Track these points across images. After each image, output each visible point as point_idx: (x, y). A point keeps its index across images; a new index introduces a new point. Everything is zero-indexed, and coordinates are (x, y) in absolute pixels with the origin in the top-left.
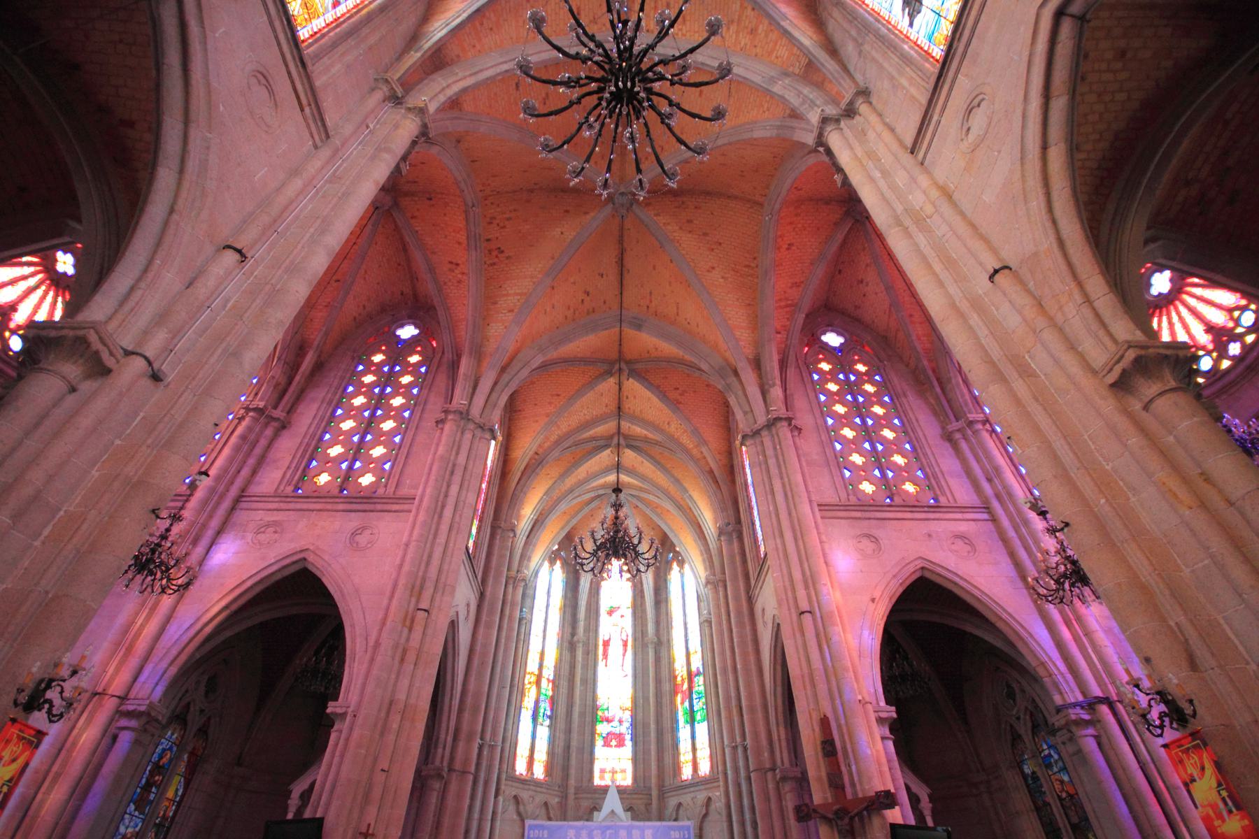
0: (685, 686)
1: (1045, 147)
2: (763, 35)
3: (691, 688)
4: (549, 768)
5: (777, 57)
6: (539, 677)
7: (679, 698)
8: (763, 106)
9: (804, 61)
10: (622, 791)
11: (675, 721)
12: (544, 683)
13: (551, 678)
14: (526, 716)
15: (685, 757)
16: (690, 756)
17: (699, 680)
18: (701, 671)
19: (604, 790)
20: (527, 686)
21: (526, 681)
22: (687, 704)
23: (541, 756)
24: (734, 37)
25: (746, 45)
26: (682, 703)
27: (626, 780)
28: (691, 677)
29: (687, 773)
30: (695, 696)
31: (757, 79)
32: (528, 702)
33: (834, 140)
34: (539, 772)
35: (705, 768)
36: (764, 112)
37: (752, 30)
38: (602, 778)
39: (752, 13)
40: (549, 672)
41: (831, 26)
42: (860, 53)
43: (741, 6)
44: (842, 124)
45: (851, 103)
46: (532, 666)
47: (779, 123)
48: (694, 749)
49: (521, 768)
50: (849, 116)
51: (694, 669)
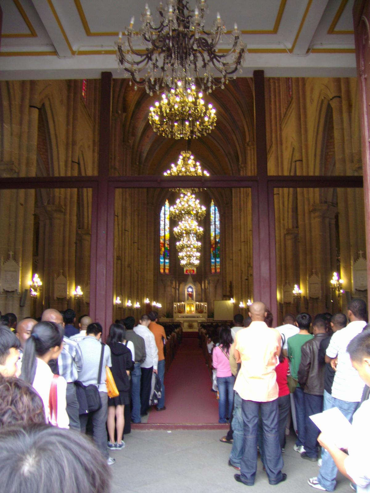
0: (214, 246)
3: (216, 246)
4: (170, 270)
6: (164, 244)
7: (212, 249)
10: (192, 275)
11: (210, 256)
12: (166, 245)
13: (168, 243)
14: (162, 256)
15: (213, 267)
16: (214, 267)
17: (219, 245)
18: (219, 242)
19: (188, 275)
20: (161, 248)
21: (161, 246)
22: (214, 252)
23: (167, 267)
26: (213, 251)
27: (195, 271)
28: (216, 243)
29: (213, 271)
30: (217, 250)
32: (162, 253)
34: (167, 271)
35: (218, 270)
38: (187, 272)
40: (167, 242)
46: (162, 241)
48: (216, 265)
49: (162, 271)
51: (217, 240)
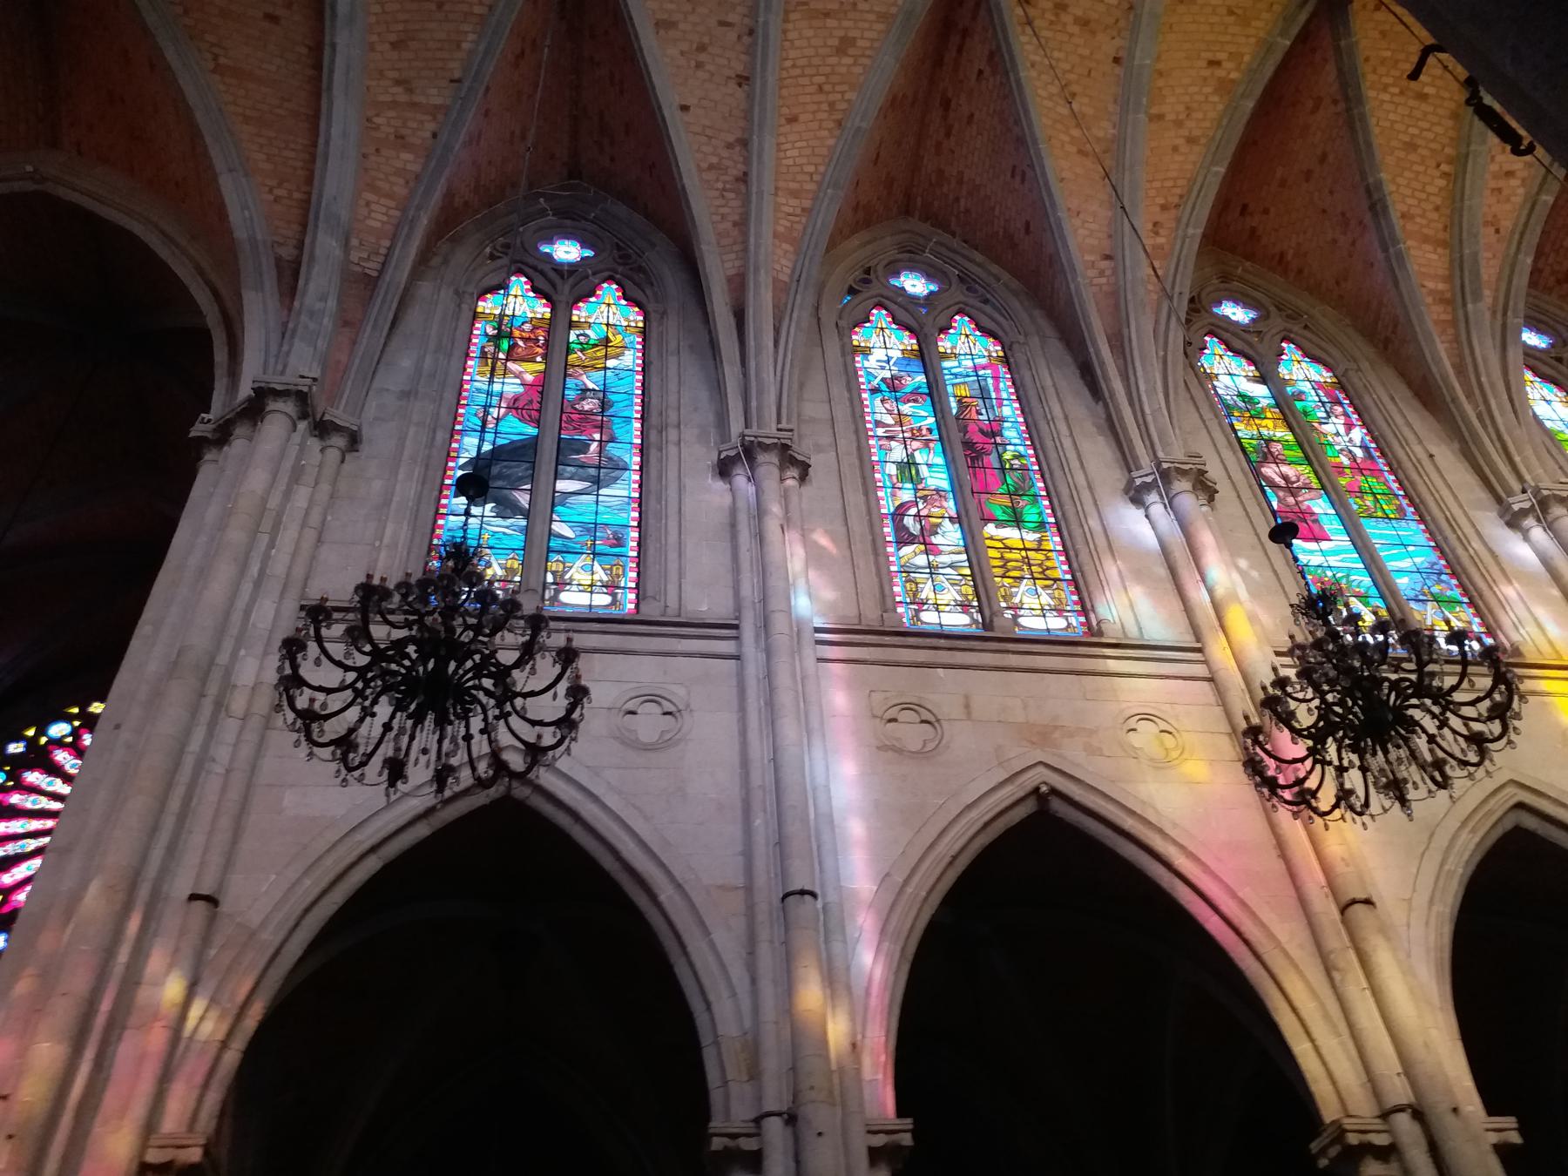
1: (373, 849)
2: (399, 164)
5: (368, 204)
8: (280, 185)
9: (372, 267)
24: (388, 98)
25: (377, 128)
31: (330, 188)
33: (276, 426)
36: (271, 191)
37: (402, 137)
39: (428, 134)
41: (425, 288)
42: (406, 395)
43: (436, 107)
44: (302, 426)
45: (338, 429)
47: (259, 237)
50: (315, 428)
